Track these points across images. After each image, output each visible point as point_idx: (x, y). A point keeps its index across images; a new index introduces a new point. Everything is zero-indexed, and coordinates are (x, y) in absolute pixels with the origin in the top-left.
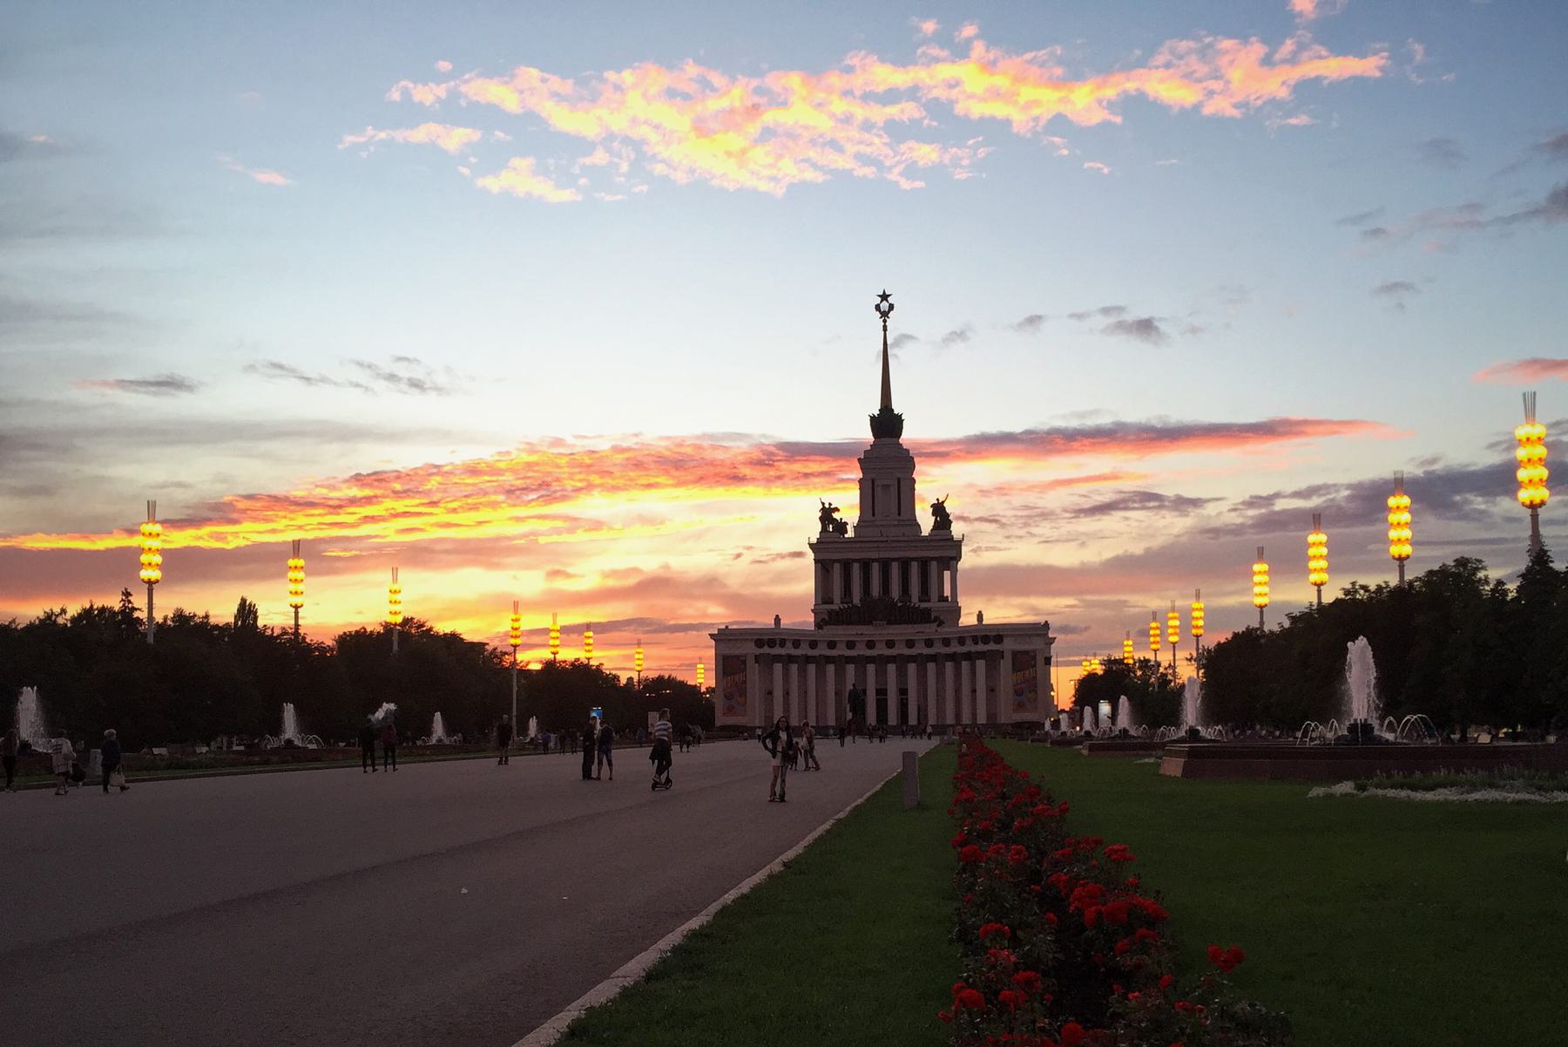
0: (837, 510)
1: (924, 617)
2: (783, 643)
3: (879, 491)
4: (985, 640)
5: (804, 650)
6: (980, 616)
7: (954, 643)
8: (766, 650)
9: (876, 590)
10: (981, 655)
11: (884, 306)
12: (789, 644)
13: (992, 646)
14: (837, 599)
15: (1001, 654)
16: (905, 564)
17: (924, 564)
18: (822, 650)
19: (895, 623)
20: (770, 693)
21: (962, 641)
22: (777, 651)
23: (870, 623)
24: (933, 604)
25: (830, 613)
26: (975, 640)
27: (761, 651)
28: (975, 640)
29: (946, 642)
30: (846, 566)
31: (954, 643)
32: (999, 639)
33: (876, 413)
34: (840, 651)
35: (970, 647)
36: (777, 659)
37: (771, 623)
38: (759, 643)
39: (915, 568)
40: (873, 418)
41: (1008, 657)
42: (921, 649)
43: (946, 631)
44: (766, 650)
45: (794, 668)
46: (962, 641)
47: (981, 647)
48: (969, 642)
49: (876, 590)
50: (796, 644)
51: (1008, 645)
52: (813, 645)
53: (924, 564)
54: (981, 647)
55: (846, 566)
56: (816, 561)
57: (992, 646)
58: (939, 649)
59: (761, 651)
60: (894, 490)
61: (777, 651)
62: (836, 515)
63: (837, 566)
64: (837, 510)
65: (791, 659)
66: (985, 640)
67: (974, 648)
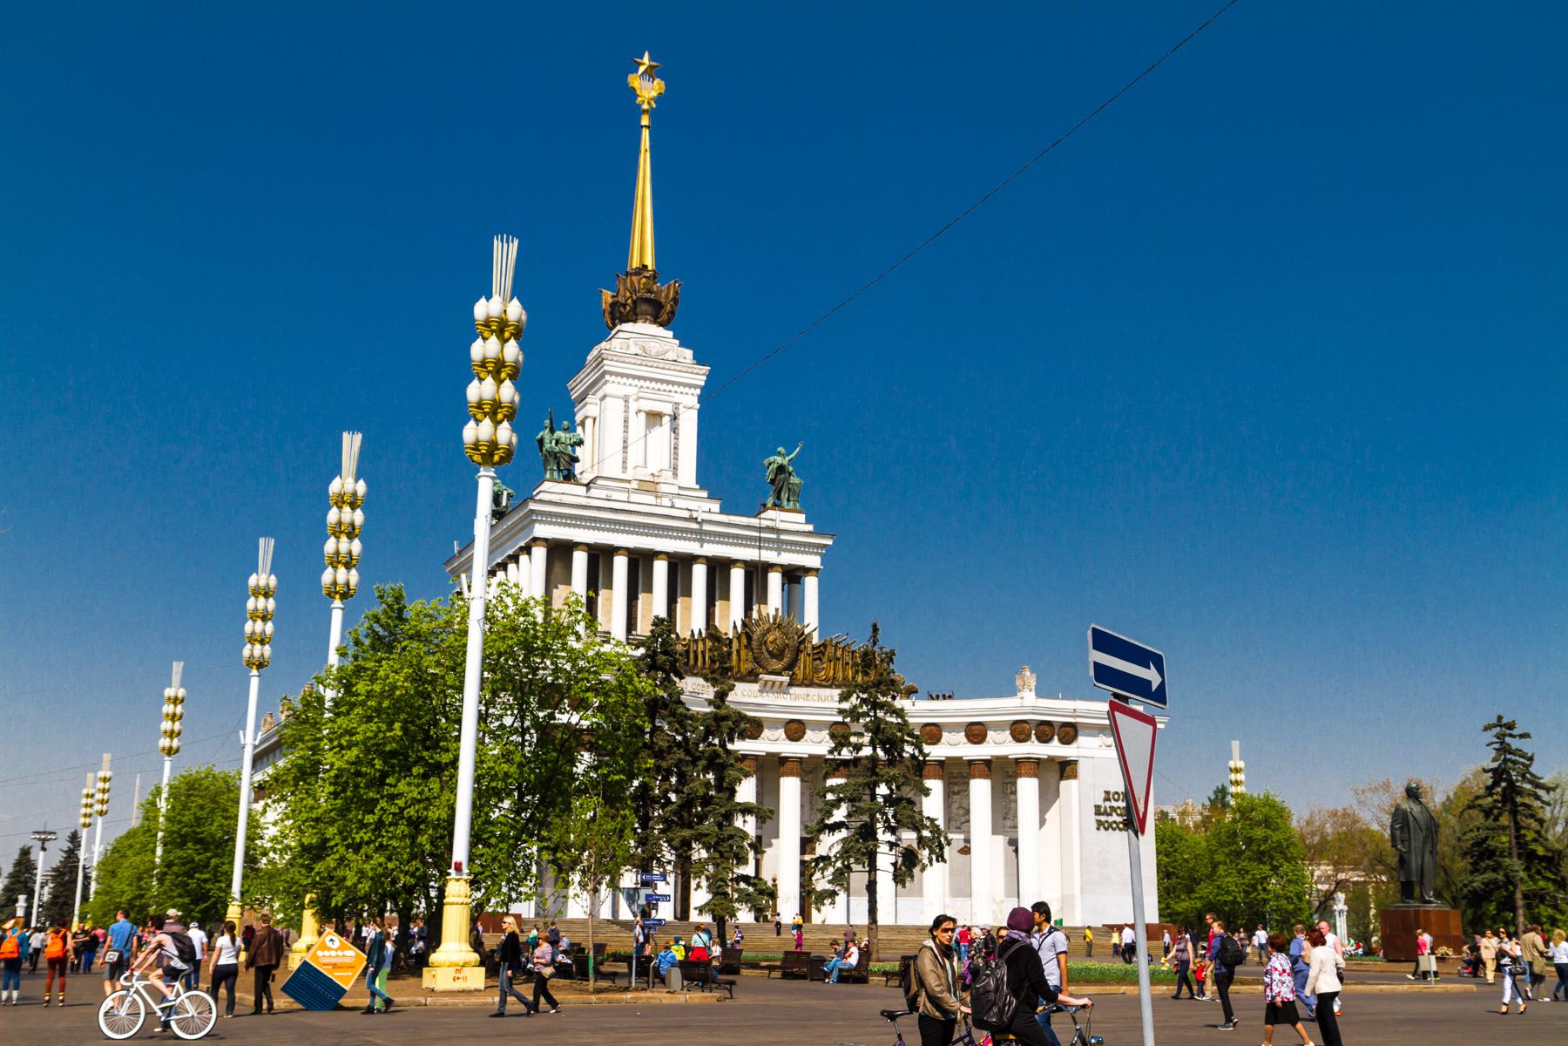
4: (1045, 730)
13: (1055, 749)
26: (1019, 731)
28: (1019, 731)
32: (1069, 733)
35: (999, 745)
57: (1055, 749)
66: (1045, 730)
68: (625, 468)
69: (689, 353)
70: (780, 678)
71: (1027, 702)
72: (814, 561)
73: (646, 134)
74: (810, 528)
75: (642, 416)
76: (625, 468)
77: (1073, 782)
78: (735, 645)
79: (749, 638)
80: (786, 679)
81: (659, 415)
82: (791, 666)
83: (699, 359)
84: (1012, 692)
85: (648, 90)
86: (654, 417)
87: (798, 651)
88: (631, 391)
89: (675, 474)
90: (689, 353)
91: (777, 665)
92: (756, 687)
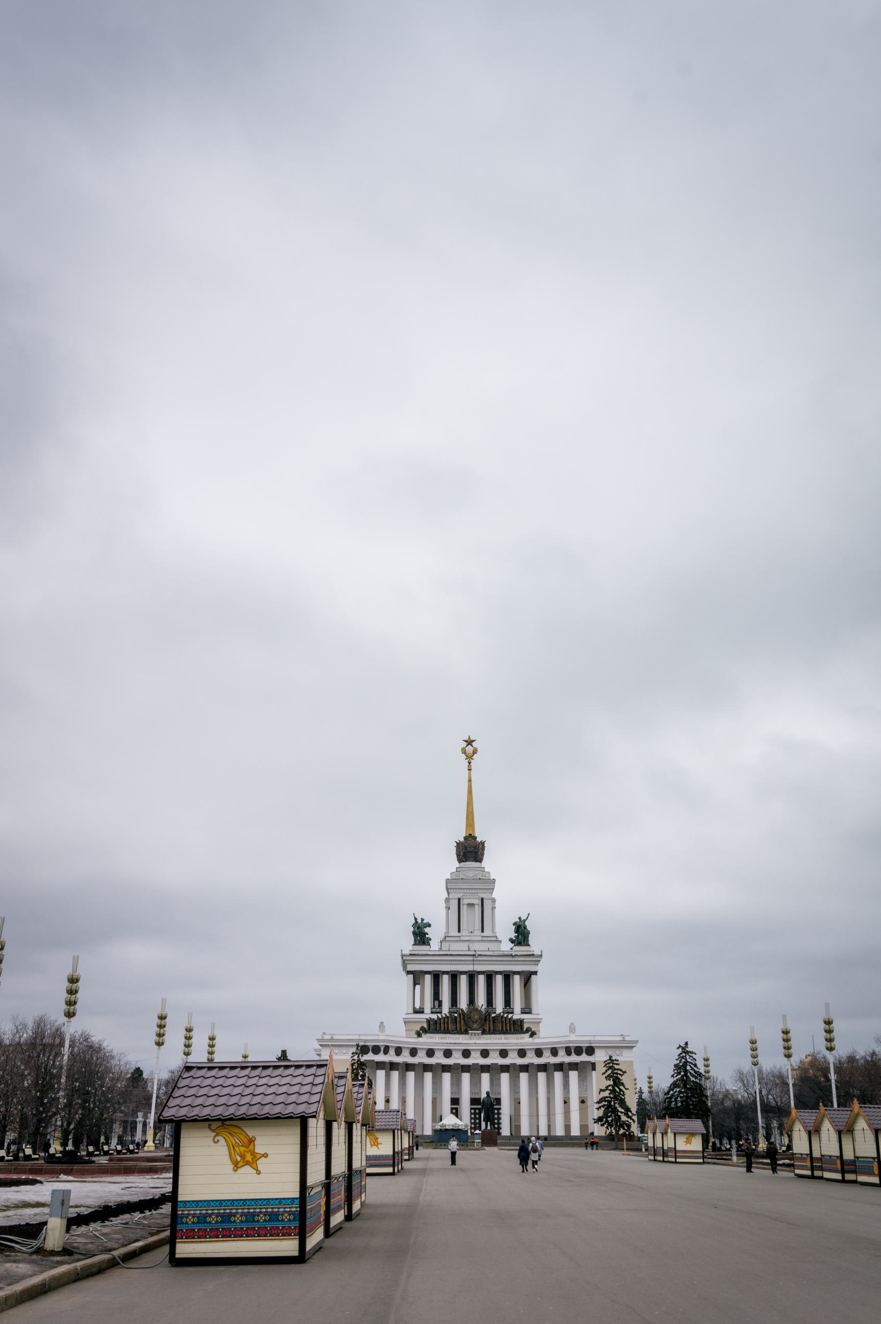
0: (429, 926)
1: (517, 1027)
2: (386, 1051)
3: (464, 909)
4: (578, 1051)
5: (405, 1058)
6: (572, 1029)
8: (370, 1057)
9: (463, 1003)
10: (574, 1066)
11: (470, 749)
12: (392, 1052)
13: (584, 1058)
14: (428, 1008)
15: (593, 1066)
16: (490, 977)
17: (507, 977)
18: (421, 1058)
19: (490, 1033)
21: (554, 1052)
22: (381, 1057)
23: (466, 1032)
24: (517, 1015)
25: (429, 1021)
28: (568, 1051)
29: (539, 1053)
30: (436, 977)
32: (590, 1051)
33: (462, 840)
34: (439, 1059)
35: (562, 1058)
36: (380, 1065)
37: (376, 1030)
38: (364, 1050)
39: (499, 981)
40: (459, 845)
41: (601, 1068)
42: (513, 1059)
43: (537, 1042)
44: (370, 1057)
45: (395, 1075)
46: (554, 1052)
48: (562, 1053)
49: (463, 1003)
50: (398, 1051)
51: (600, 1057)
52: (413, 1052)
53: (507, 977)
55: (436, 977)
56: (409, 973)
57: (584, 1058)
58: (531, 1059)
60: (478, 909)
61: (381, 1057)
62: (427, 930)
63: (428, 979)
64: (429, 926)
65: (393, 1066)
66: (578, 1051)
67: (567, 1059)
68: (459, 931)
75: (465, 906)
76: (459, 931)
78: (458, 1019)
81: (473, 905)
82: (483, 1025)
86: (471, 905)
87: (486, 1020)
88: (459, 896)
89: (483, 931)
91: (475, 1026)
92: (466, 1036)
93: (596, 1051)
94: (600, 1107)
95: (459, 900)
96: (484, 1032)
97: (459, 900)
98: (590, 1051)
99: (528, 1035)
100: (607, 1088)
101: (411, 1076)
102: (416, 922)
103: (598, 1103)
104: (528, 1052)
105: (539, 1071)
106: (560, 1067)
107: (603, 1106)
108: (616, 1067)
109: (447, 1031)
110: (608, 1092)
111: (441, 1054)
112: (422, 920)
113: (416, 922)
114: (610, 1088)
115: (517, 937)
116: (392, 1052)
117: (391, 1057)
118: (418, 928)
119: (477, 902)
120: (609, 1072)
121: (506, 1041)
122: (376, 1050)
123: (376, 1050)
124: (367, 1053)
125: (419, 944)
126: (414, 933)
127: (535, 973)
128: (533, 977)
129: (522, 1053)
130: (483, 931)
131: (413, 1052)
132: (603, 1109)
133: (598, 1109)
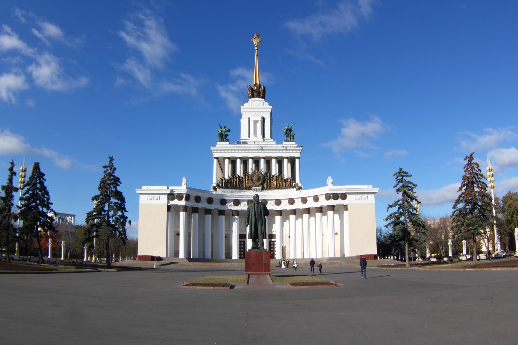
0: (229, 131)
4: (335, 196)
7: (310, 201)
8: (176, 202)
13: (340, 201)
20: (178, 234)
26: (328, 197)
27: (172, 203)
28: (328, 197)
29: (304, 200)
31: (310, 201)
32: (344, 196)
35: (323, 202)
47: (332, 202)
48: (322, 199)
50: (198, 199)
54: (332, 202)
59: (172, 203)
61: (183, 203)
62: (228, 133)
66: (335, 196)
68: (249, 137)
69: (267, 103)
70: (258, 188)
71: (330, 188)
72: (298, 155)
73: (256, 51)
74: (297, 145)
76: (249, 137)
77: (346, 213)
78: (244, 179)
79: (248, 177)
80: (260, 188)
83: (270, 105)
84: (326, 185)
85: (255, 41)
86: (256, 122)
89: (264, 137)
90: (267, 103)
93: (348, 196)
94: (389, 224)
95: (249, 118)
96: (263, 189)
97: (249, 118)
98: (344, 196)
99: (295, 189)
100: (396, 203)
101: (209, 217)
102: (221, 128)
103: (387, 220)
104: (296, 200)
105: (304, 213)
106: (320, 209)
107: (392, 223)
108: (407, 179)
109: (235, 188)
110: (397, 207)
111: (232, 203)
112: (225, 127)
113: (221, 128)
114: (401, 202)
115: (287, 137)
116: (192, 198)
117: (193, 204)
118: (222, 131)
119: (260, 119)
120: (400, 184)
121: (279, 194)
122: (180, 197)
123: (180, 197)
124: (173, 199)
125: (222, 141)
126: (219, 135)
127: (299, 158)
128: (297, 161)
129: (292, 201)
130: (264, 137)
131: (210, 201)
132: (392, 226)
133: (387, 226)
